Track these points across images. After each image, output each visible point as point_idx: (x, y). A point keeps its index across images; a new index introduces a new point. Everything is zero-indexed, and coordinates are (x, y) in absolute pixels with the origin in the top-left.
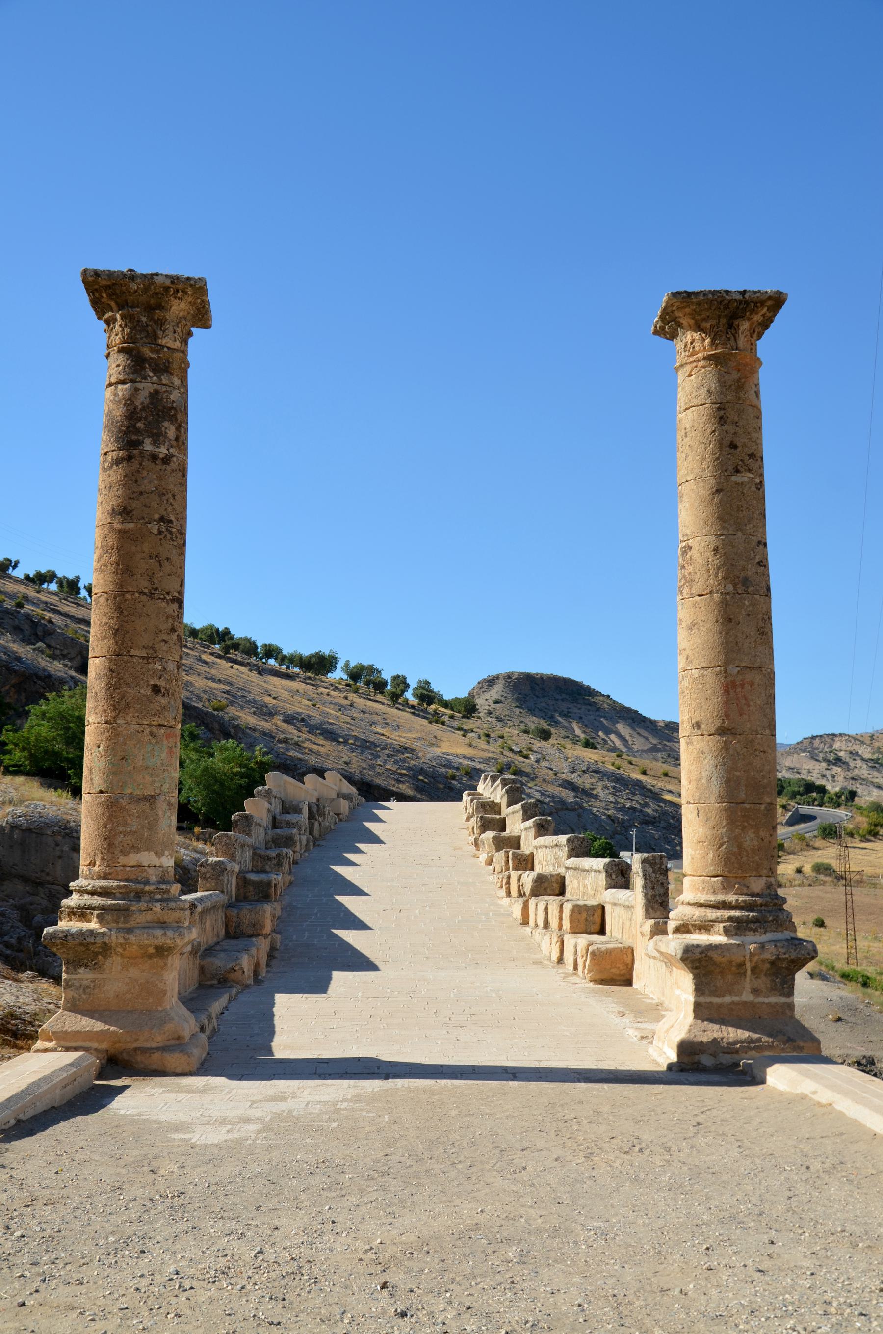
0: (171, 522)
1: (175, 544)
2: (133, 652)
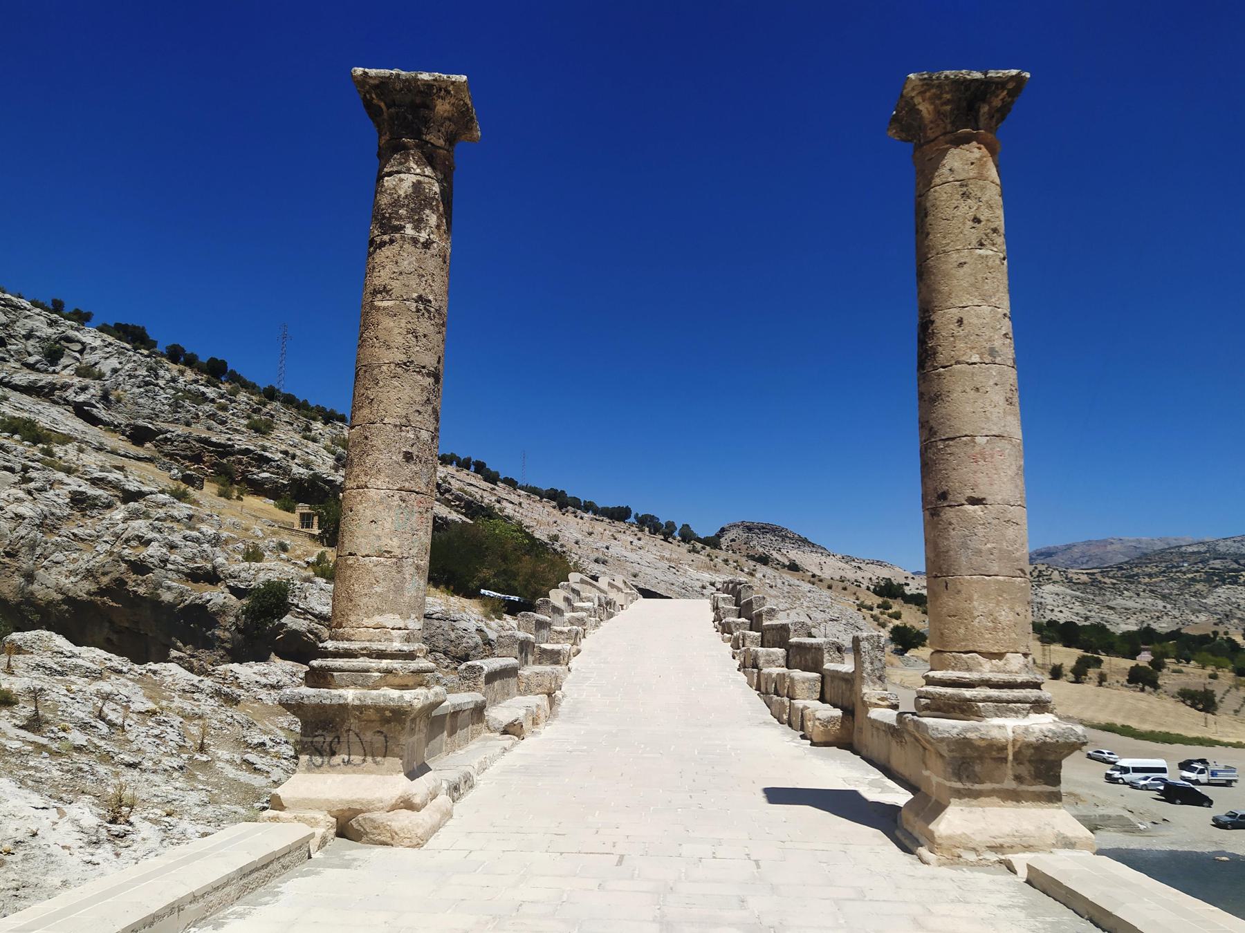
0: (430, 301)
1: (433, 322)
2: (386, 420)
